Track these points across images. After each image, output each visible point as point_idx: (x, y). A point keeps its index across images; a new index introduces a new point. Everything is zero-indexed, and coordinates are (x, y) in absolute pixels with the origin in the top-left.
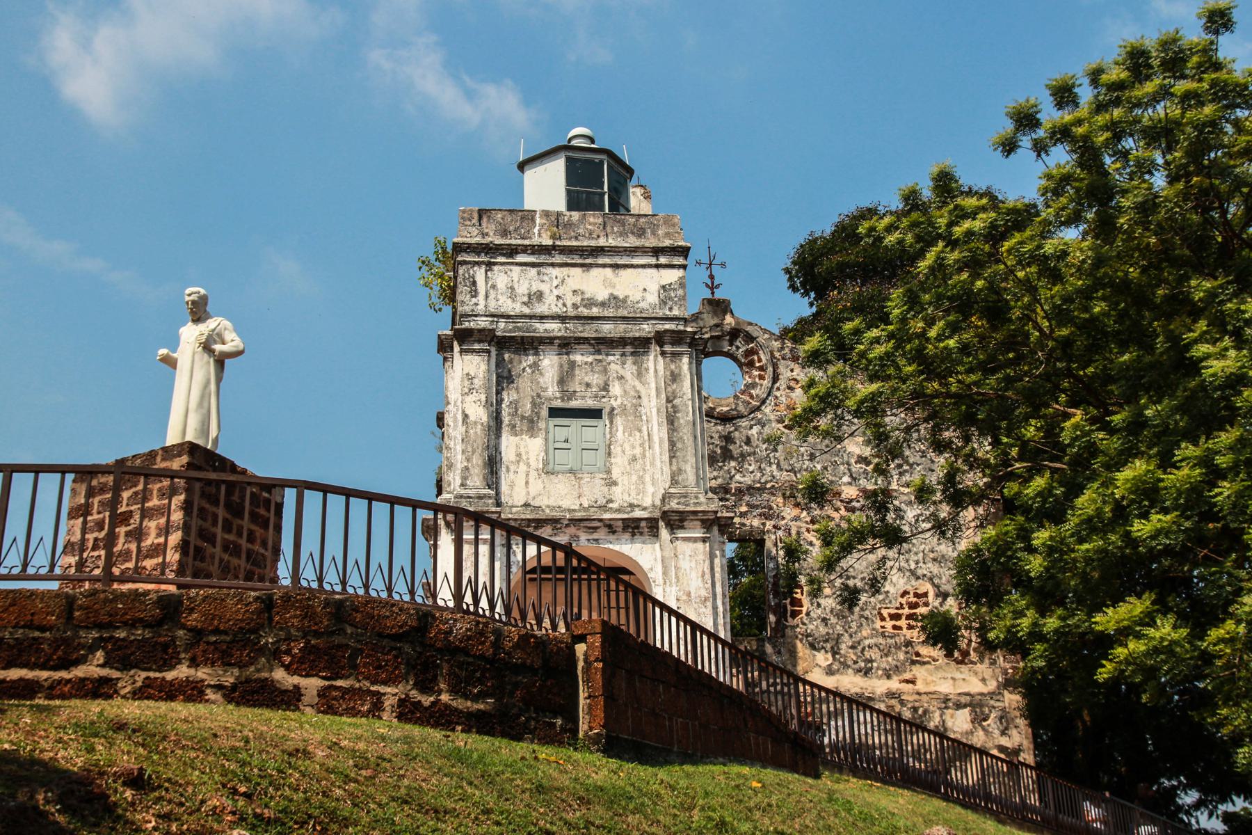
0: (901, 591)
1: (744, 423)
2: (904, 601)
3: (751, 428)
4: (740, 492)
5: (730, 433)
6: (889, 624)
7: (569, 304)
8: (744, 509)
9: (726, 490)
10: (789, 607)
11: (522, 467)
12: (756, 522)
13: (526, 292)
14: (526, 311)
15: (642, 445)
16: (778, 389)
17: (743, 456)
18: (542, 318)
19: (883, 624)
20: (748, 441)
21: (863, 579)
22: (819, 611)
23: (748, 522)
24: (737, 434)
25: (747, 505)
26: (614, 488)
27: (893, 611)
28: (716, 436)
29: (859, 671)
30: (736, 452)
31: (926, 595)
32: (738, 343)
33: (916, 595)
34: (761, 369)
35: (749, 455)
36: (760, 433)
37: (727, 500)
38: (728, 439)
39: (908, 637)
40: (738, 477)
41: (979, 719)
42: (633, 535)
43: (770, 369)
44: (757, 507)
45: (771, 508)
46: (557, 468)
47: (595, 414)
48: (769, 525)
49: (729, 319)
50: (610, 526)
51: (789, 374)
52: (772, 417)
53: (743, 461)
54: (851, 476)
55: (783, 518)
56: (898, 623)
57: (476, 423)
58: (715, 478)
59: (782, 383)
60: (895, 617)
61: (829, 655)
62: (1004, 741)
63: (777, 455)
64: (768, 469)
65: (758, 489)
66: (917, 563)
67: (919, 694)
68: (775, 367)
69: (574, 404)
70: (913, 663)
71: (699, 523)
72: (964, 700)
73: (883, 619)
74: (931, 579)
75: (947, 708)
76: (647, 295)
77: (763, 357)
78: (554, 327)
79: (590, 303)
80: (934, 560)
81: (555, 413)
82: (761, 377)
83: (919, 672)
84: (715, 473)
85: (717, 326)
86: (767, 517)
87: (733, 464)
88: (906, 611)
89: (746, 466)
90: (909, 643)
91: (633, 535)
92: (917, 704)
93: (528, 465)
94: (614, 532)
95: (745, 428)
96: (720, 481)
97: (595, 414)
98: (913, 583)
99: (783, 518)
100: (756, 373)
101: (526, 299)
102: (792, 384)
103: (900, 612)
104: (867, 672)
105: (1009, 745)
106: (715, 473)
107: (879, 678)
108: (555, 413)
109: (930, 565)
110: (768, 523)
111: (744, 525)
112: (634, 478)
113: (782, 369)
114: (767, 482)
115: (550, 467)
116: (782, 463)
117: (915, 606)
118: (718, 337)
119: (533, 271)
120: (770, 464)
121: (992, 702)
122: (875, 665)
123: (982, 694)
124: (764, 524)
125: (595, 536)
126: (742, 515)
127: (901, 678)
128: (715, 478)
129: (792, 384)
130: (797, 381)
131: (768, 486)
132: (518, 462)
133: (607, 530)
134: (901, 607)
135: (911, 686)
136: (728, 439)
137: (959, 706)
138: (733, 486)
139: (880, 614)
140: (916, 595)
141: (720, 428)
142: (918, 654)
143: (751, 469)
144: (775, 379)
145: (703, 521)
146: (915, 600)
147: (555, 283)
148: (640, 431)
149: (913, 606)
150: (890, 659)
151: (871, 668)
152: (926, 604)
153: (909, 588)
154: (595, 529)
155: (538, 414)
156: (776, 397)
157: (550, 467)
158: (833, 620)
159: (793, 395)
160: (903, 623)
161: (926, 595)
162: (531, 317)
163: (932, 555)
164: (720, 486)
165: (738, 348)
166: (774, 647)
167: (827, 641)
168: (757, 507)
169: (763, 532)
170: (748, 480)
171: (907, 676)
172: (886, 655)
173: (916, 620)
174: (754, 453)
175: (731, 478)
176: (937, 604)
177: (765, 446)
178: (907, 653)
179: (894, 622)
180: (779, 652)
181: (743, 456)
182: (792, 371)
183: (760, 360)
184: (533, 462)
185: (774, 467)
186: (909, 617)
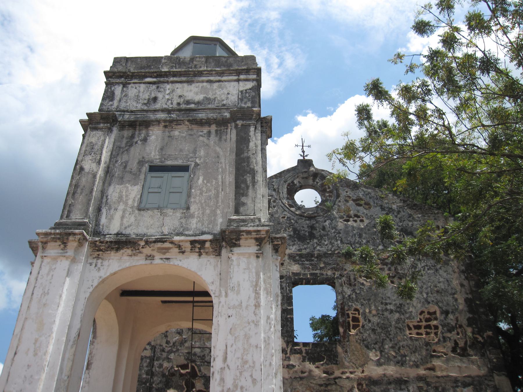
0: (419, 312)
1: (321, 219)
2: (422, 317)
3: (325, 221)
4: (319, 257)
5: (313, 224)
6: (414, 331)
7: (175, 103)
8: (322, 265)
9: (312, 256)
10: (351, 323)
11: (121, 207)
12: (330, 273)
13: (147, 97)
14: (145, 108)
15: (216, 189)
16: (340, 201)
17: (321, 236)
18: (155, 111)
19: (410, 332)
20: (324, 228)
21: (395, 304)
22: (370, 325)
23: (325, 273)
24: (317, 225)
25: (324, 263)
26: (191, 220)
27: (416, 324)
28: (306, 226)
29: (398, 362)
30: (317, 235)
31: (435, 313)
32: (317, 180)
33: (429, 313)
34: (331, 192)
35: (325, 236)
36: (330, 224)
37: (313, 260)
38: (312, 227)
39: (427, 340)
40: (318, 248)
42: (200, 254)
43: (335, 191)
44: (330, 264)
45: (338, 265)
46: (148, 206)
47: (184, 169)
48: (337, 274)
49: (312, 169)
50: (179, 247)
51: (345, 193)
52: (337, 216)
53: (321, 239)
54: (384, 246)
55: (346, 270)
56: (420, 331)
57: (88, 173)
58: (305, 249)
59: (342, 198)
60: (418, 327)
61: (378, 353)
63: (341, 235)
64: (336, 243)
65: (330, 254)
66: (427, 294)
67: (438, 377)
68: (337, 190)
69: (169, 163)
70: (432, 356)
71: (253, 241)
72: (468, 380)
73: (410, 329)
74: (437, 303)
75: (457, 386)
76: (229, 96)
77: (331, 186)
78: (162, 116)
79: (188, 102)
80: (438, 292)
81: (153, 169)
82: (330, 196)
83: (436, 363)
84: (305, 246)
85: (306, 172)
86: (336, 269)
87: (315, 241)
88: (424, 323)
89: (323, 242)
90: (427, 344)
91: (200, 254)
92: (438, 385)
93: (126, 204)
94: (183, 252)
95: (322, 222)
96: (308, 250)
97: (184, 169)
98: (426, 306)
99: (346, 270)
100: (327, 194)
101: (146, 102)
102: (347, 198)
103: (420, 324)
104: (401, 363)
106: (305, 246)
107: (411, 367)
108: (153, 169)
109: (435, 295)
110: (336, 273)
111: (322, 274)
112: (208, 211)
113: (341, 191)
114: (335, 250)
115: (142, 205)
116: (344, 239)
117: (428, 320)
118: (306, 178)
119: (154, 87)
120: (337, 240)
121: (486, 382)
122: (408, 358)
123: (478, 376)
124: (334, 274)
125: (167, 256)
126: (321, 269)
127: (425, 367)
128: (305, 249)
129: (347, 198)
130: (349, 197)
131: (336, 252)
132: (119, 202)
133: (177, 250)
134: (421, 321)
135: (432, 373)
136: (312, 227)
138: (316, 252)
139: (408, 326)
140: (429, 313)
141: (308, 222)
142: (434, 351)
143: (326, 243)
144: (338, 196)
145: (256, 239)
146: (428, 316)
147: (168, 92)
148: (216, 179)
149: (428, 320)
150: (417, 354)
151: (405, 361)
152: (436, 319)
153: (423, 309)
154: (168, 249)
155: (140, 171)
156: (339, 206)
157: (142, 205)
158: (379, 330)
159: (348, 204)
160: (423, 331)
161: (435, 313)
162: (147, 111)
163: (436, 289)
164: (308, 254)
165: (317, 183)
166: (343, 347)
167: (376, 343)
168: (330, 264)
169: (334, 278)
170: (324, 249)
171: (429, 365)
172: (414, 352)
173: (431, 328)
174: (328, 235)
175: (315, 248)
176: (442, 318)
177: (333, 231)
178: (427, 350)
179: (417, 331)
180: (346, 352)
181: (321, 236)
182: (347, 192)
183: (329, 188)
184: (130, 202)
185: (339, 242)
186: (426, 327)
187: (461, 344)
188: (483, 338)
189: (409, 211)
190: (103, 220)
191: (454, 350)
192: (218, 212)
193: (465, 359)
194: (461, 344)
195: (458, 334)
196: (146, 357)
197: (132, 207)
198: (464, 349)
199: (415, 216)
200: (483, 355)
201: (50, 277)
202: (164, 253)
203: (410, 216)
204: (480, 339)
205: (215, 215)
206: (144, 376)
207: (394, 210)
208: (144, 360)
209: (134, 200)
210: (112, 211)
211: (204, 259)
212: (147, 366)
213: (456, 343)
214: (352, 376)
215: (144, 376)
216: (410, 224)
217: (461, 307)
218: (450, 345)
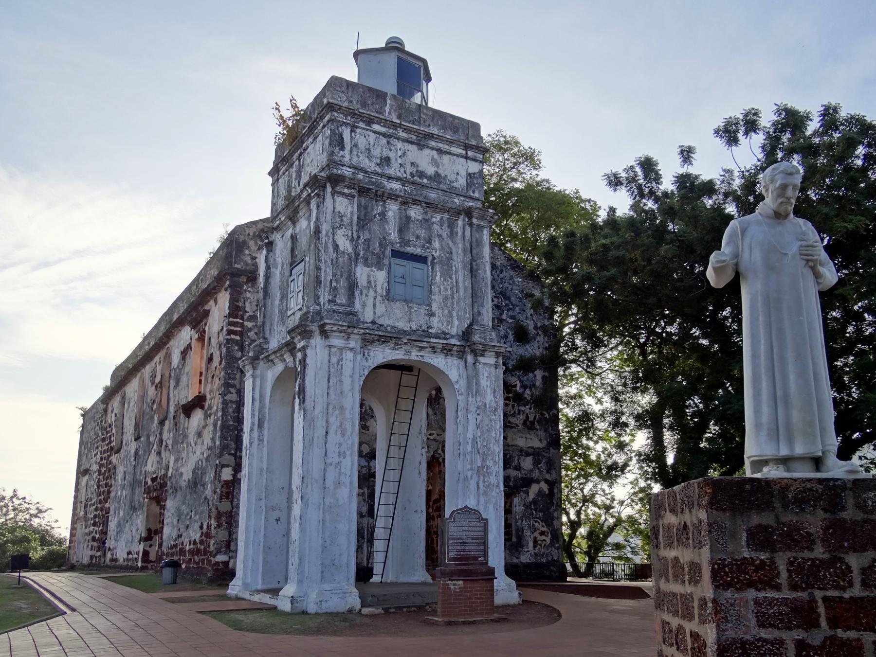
7: (408, 172)
13: (379, 155)
14: (379, 170)
15: (452, 289)
18: (390, 178)
26: (433, 318)
41: (536, 463)
42: (447, 355)
57: (344, 252)
62: (548, 477)
69: (409, 249)
71: (494, 354)
72: (530, 451)
76: (459, 177)
78: (395, 186)
79: (422, 174)
81: (396, 254)
91: (447, 355)
93: (376, 292)
94: (435, 352)
101: (378, 161)
105: (550, 479)
108: (396, 254)
112: (446, 312)
119: (384, 141)
123: (539, 448)
132: (369, 288)
137: (528, 454)
142: (509, 422)
145: (496, 352)
147: (399, 153)
148: (451, 278)
155: (384, 252)
162: (382, 175)
180: (435, 414)
184: (379, 289)
187: (531, 418)
188: (549, 415)
189: (512, 273)
190: (358, 306)
191: (525, 423)
192: (455, 314)
193: (531, 432)
194: (531, 418)
195: (530, 409)
196: (231, 402)
197: (382, 296)
198: (532, 423)
199: (516, 280)
200: (546, 430)
201: (340, 367)
202: (420, 351)
203: (511, 278)
204: (547, 415)
205: (452, 317)
206: (231, 423)
207: (497, 268)
208: (230, 405)
209: (382, 288)
210: (364, 296)
211: (450, 359)
212: (233, 412)
213: (527, 417)
214: (438, 438)
215: (231, 423)
216: (510, 287)
217: (538, 384)
218: (522, 417)
